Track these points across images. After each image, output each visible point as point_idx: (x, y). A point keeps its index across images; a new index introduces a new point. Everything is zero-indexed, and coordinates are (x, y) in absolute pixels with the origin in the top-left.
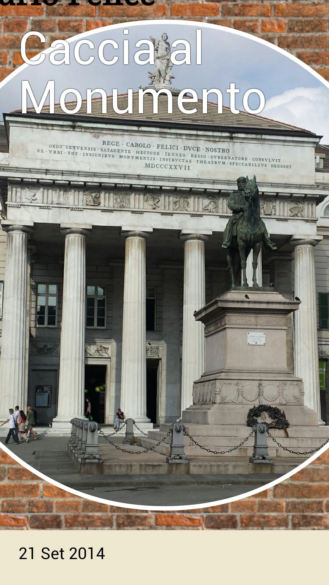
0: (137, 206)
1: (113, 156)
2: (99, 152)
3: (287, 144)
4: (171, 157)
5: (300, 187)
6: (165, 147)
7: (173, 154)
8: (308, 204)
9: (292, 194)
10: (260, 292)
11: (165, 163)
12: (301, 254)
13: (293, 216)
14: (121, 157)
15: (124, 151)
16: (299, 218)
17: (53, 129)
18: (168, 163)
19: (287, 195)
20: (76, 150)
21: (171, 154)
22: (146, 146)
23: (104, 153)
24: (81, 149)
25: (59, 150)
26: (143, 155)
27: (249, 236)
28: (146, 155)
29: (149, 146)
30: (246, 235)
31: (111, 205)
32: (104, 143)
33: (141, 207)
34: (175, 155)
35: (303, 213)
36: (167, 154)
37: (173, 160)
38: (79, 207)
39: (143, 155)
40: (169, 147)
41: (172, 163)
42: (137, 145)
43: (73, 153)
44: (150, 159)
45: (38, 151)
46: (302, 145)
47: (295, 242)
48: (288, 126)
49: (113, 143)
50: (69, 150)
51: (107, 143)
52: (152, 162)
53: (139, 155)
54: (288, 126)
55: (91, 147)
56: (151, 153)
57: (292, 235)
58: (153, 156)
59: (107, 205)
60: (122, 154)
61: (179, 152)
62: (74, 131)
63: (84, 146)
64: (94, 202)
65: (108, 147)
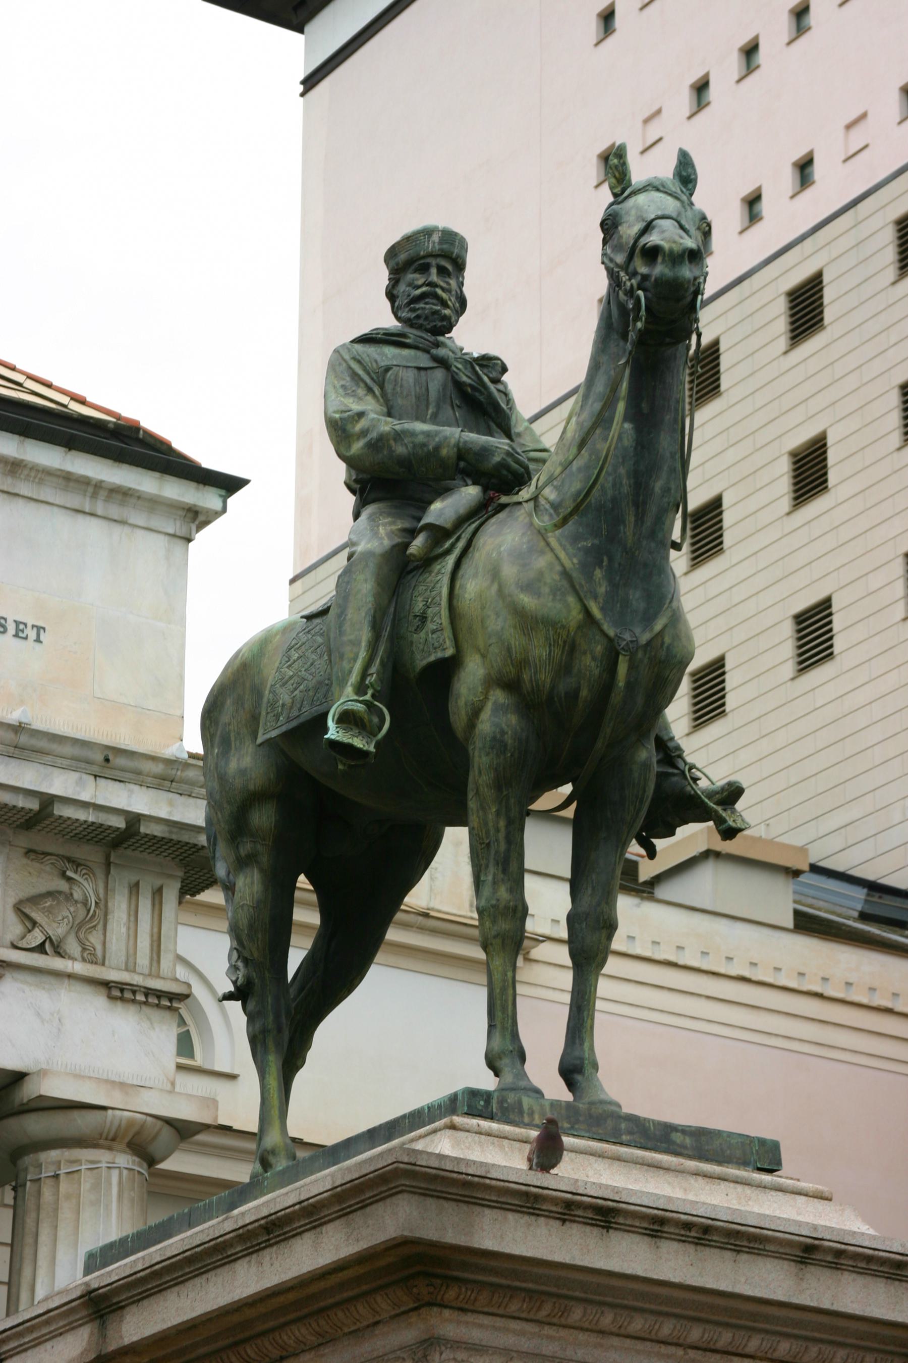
3: (24, 489)
5: (109, 762)
8: (134, 889)
9: (48, 801)
10: (692, 1164)
12: (66, 1213)
13: (40, 949)
16: (78, 968)
19: (21, 802)
27: (589, 664)
30: (571, 648)
35: (95, 939)
46: (114, 511)
47: (36, 1126)
48: (30, 385)
54: (30, 385)
57: (19, 1077)
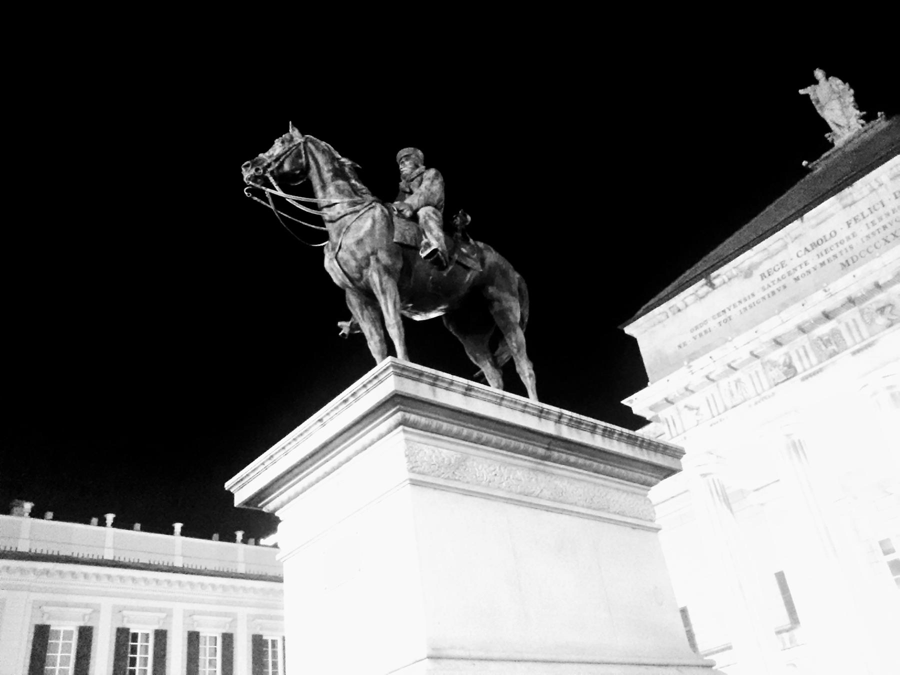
0: (858, 339)
1: (785, 287)
2: (759, 296)
4: (879, 225)
6: (861, 217)
7: (880, 219)
11: (873, 240)
14: (797, 279)
15: (799, 268)
17: (687, 306)
18: (879, 237)
20: (728, 313)
21: (877, 221)
22: (828, 237)
23: (769, 291)
24: (734, 306)
25: (705, 327)
26: (831, 254)
28: (836, 251)
29: (833, 234)
31: (814, 360)
32: (763, 276)
33: (865, 334)
34: (884, 217)
36: (870, 225)
37: (885, 227)
38: (763, 395)
39: (831, 254)
40: (866, 212)
41: (884, 234)
42: (815, 245)
43: (726, 321)
44: (844, 252)
45: (680, 347)
49: (776, 268)
50: (719, 319)
51: (767, 274)
52: (851, 253)
53: (824, 259)
55: (746, 296)
56: (842, 242)
58: (846, 244)
59: (807, 366)
60: (795, 276)
61: (888, 209)
62: (714, 289)
63: (736, 301)
64: (785, 373)
65: (771, 278)
